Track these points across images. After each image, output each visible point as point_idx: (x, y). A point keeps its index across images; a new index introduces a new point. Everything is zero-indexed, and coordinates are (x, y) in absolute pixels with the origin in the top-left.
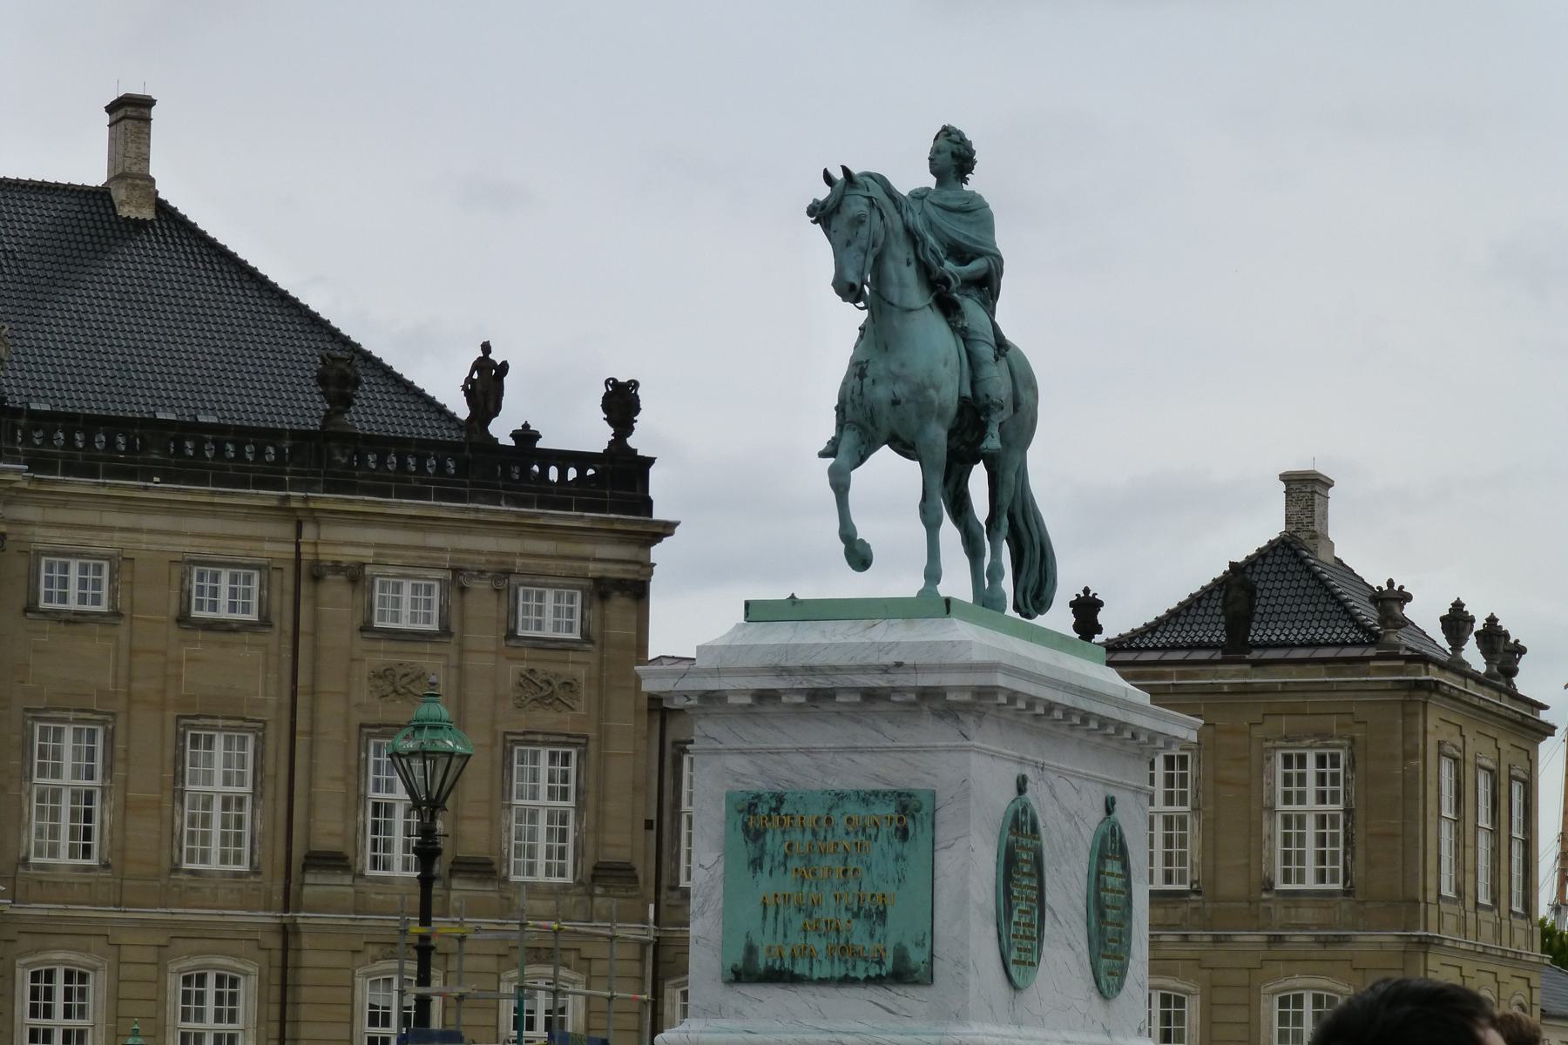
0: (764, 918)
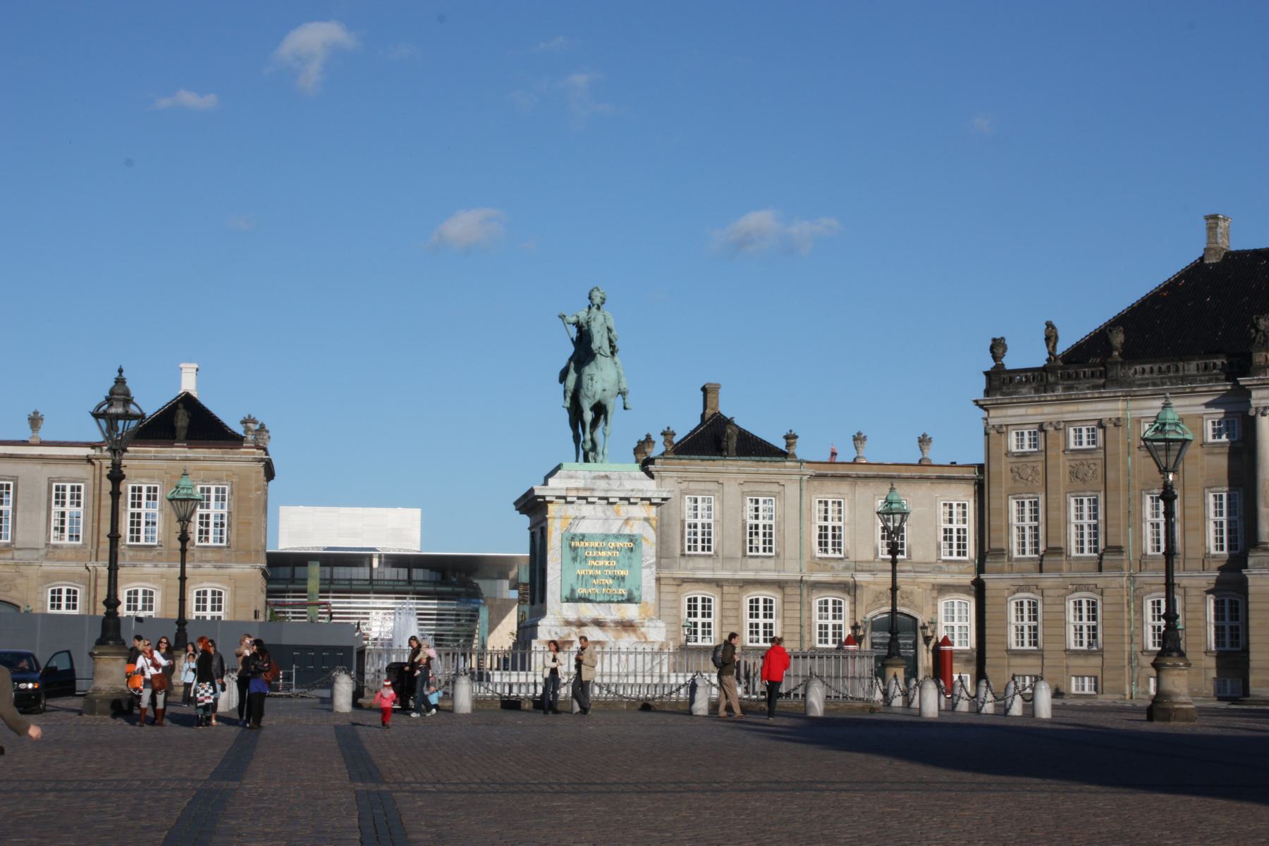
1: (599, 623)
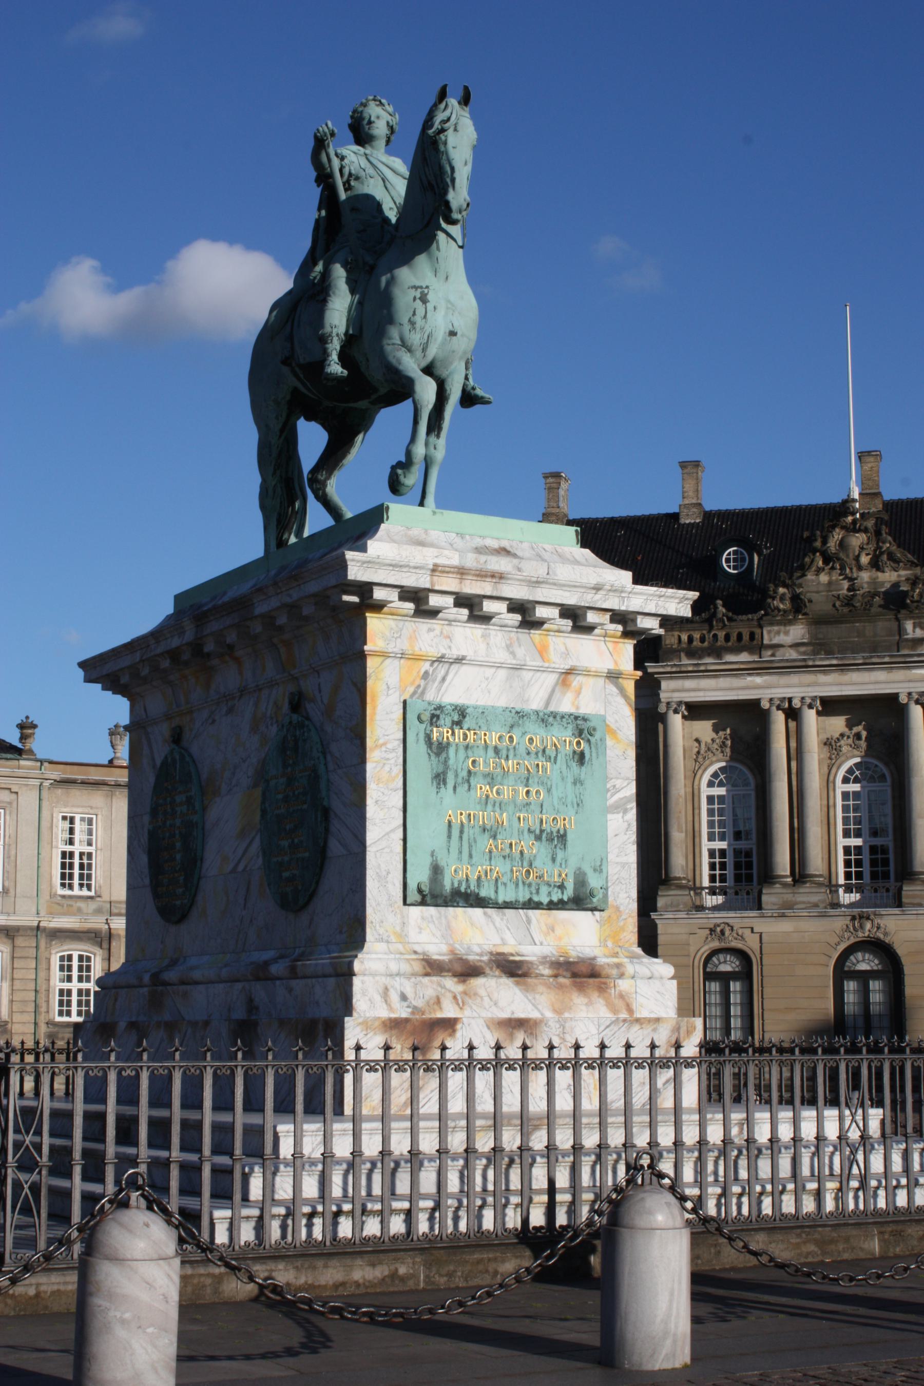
0: (449, 836)
1: (513, 969)
